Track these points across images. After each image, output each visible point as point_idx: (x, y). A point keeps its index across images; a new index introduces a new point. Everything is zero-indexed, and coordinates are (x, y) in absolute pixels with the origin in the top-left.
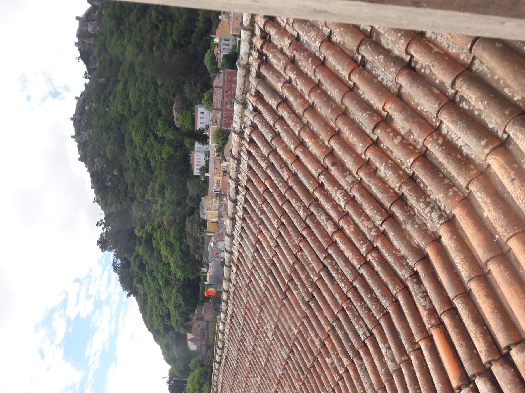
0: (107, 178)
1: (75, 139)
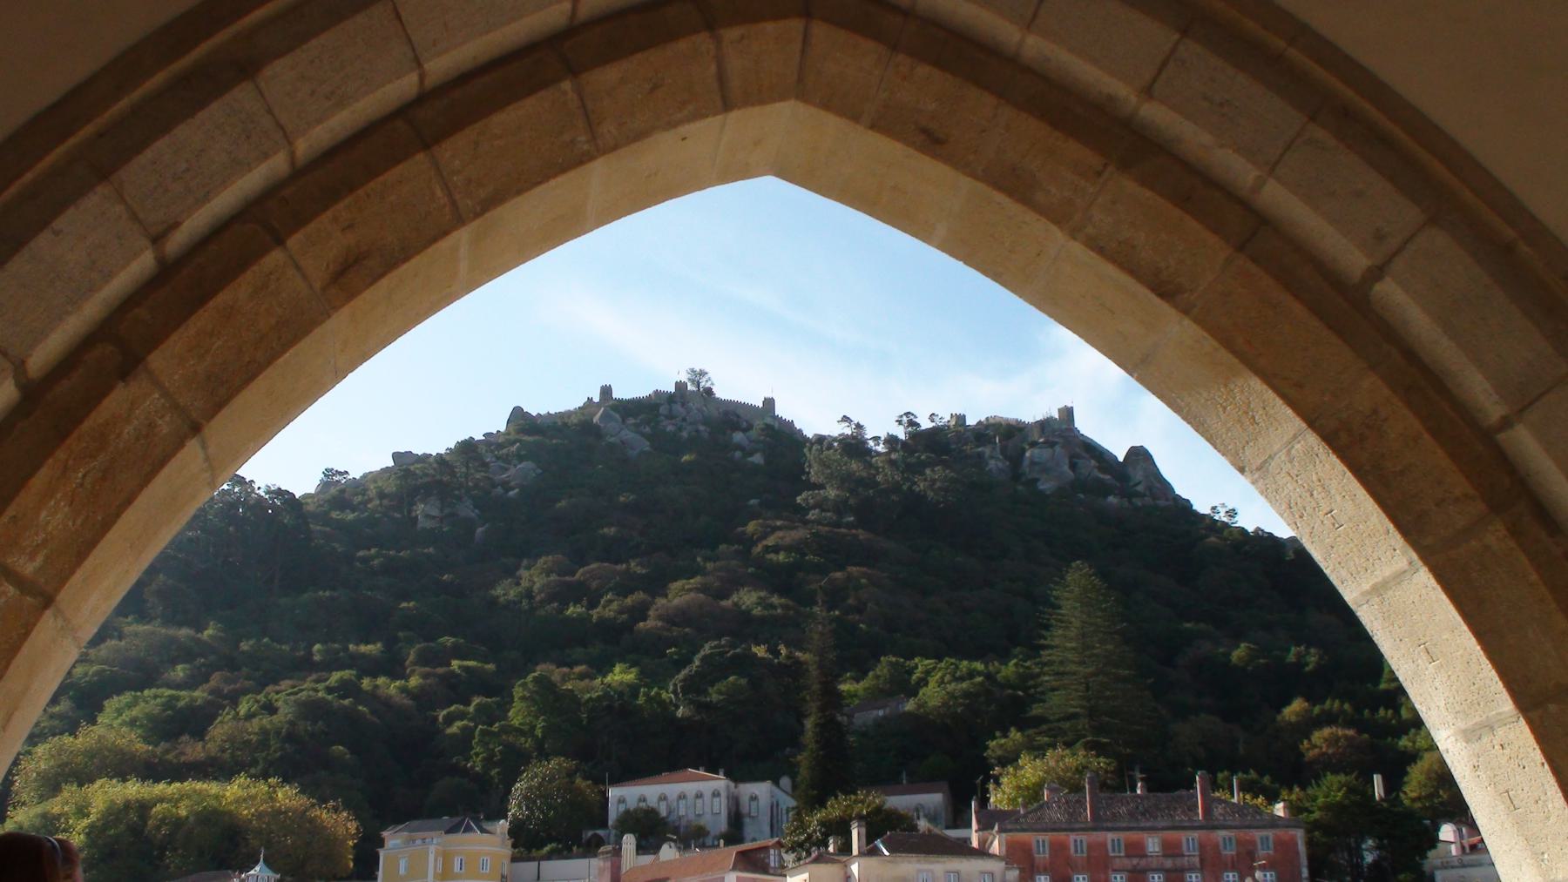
1: (596, 399)
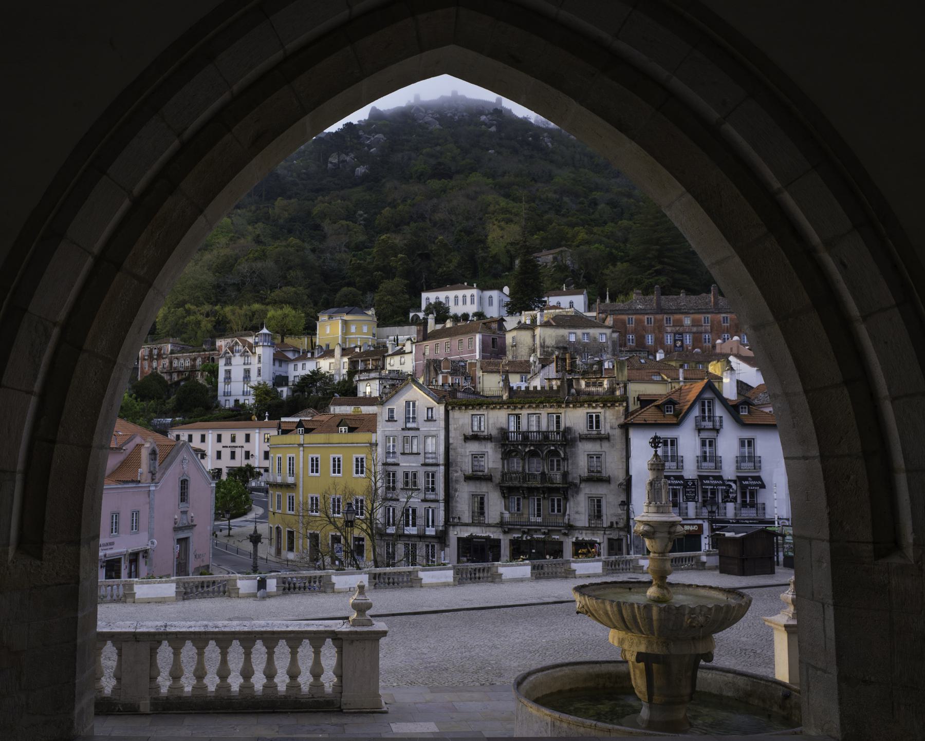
0: (347, 154)
